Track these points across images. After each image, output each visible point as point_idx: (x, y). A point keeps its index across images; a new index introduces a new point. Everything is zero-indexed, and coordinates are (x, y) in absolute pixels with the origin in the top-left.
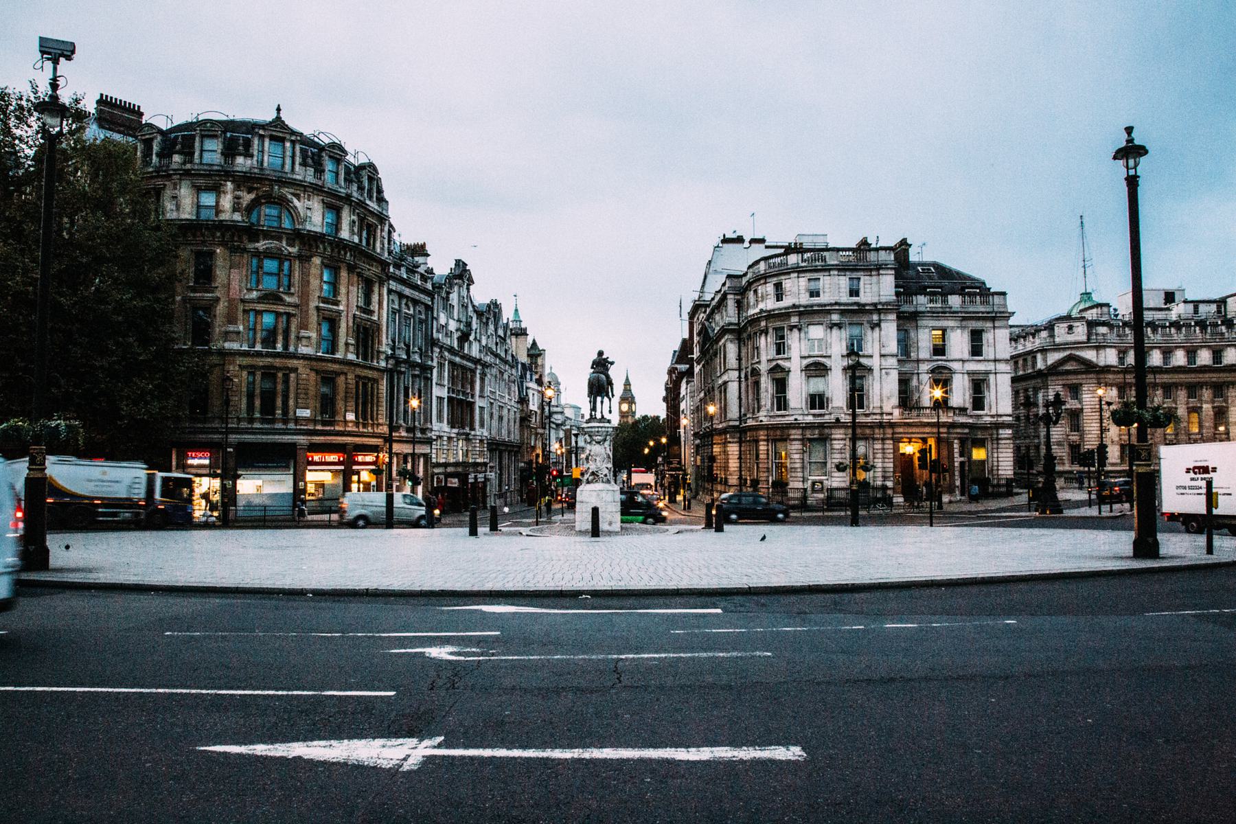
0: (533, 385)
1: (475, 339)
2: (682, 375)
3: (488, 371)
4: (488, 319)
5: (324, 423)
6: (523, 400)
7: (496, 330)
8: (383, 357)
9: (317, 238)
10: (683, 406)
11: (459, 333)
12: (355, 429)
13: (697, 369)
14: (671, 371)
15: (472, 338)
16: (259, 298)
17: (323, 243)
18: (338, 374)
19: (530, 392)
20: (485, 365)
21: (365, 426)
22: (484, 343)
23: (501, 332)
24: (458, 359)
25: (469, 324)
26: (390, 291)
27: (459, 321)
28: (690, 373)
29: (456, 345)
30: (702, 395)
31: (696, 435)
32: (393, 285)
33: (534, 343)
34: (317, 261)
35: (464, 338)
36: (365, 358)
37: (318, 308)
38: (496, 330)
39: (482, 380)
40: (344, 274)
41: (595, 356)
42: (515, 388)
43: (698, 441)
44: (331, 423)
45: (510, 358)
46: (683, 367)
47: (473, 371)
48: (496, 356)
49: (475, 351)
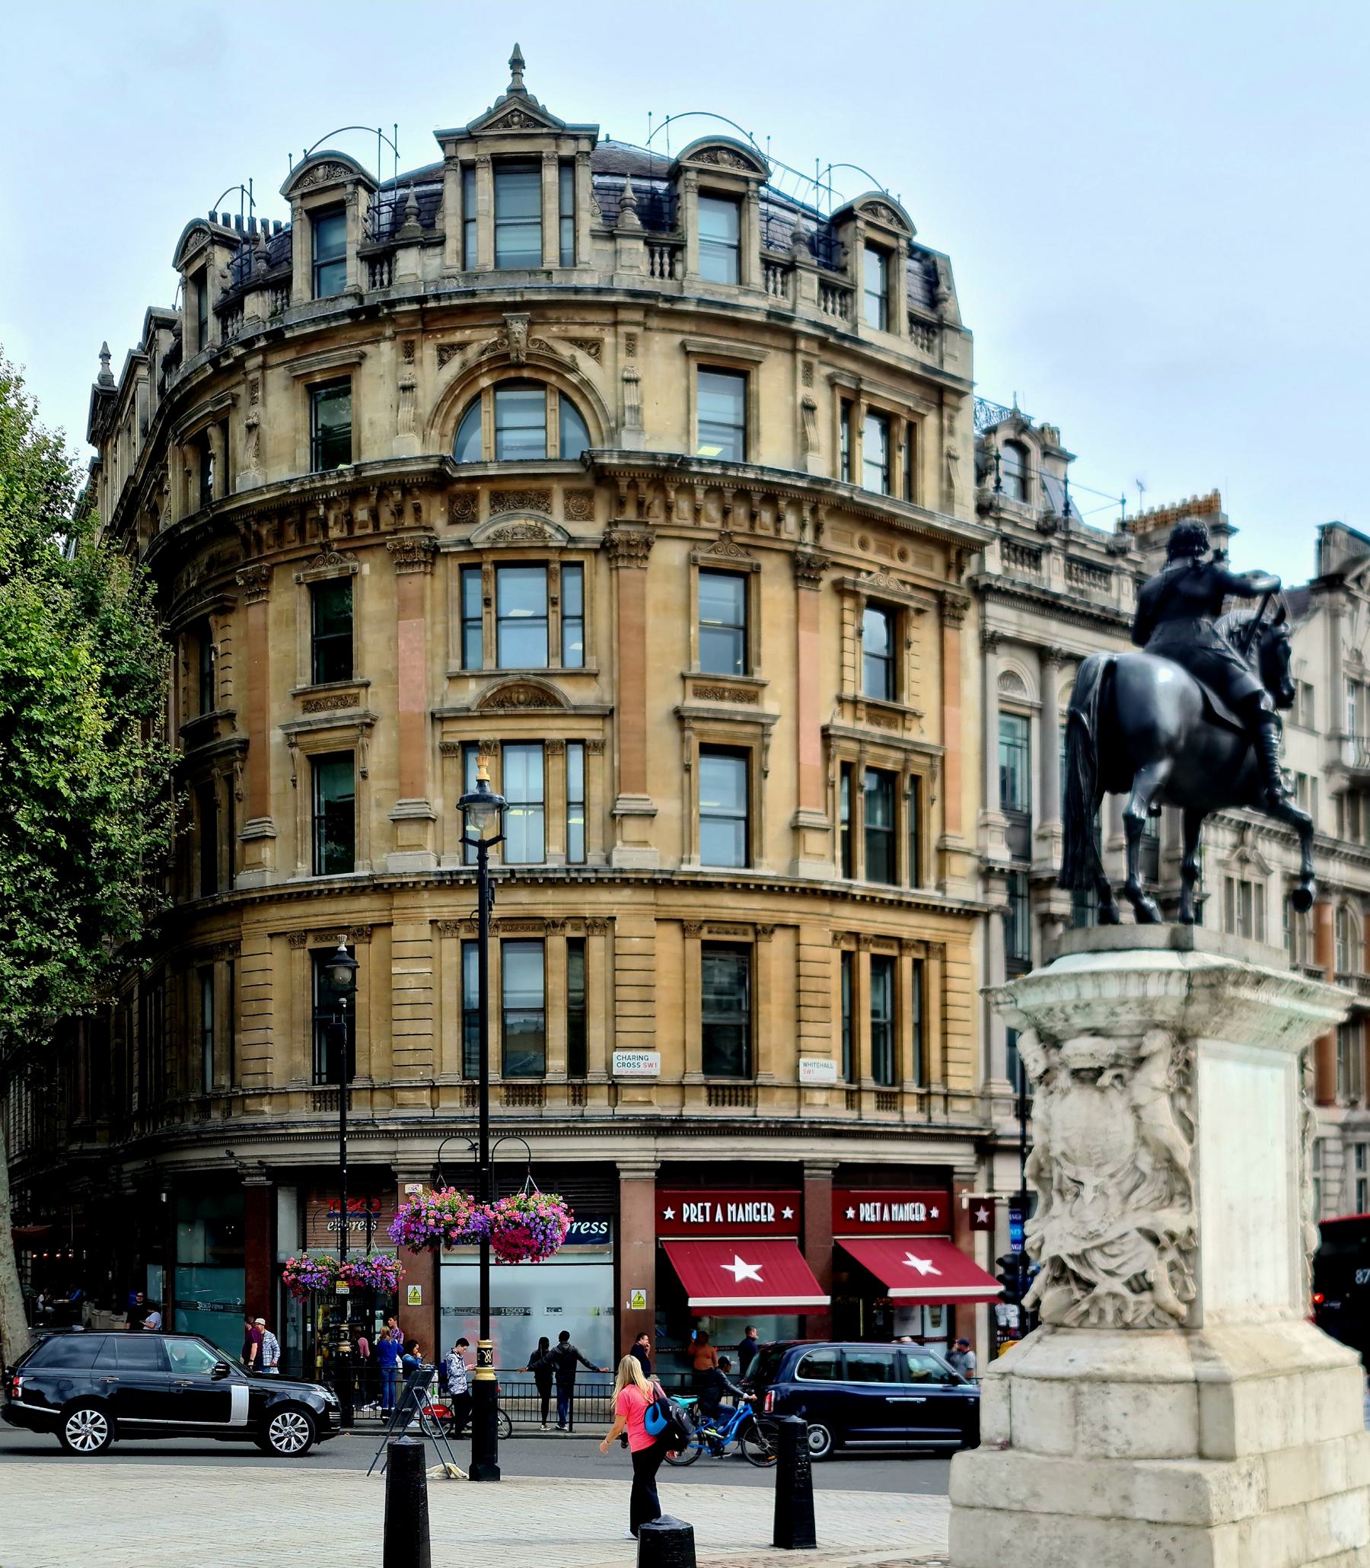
5: (717, 1095)
8: (961, 867)
9: (669, 474)
11: (1341, 782)
12: (839, 1111)
16: (485, 702)
17: (688, 489)
18: (765, 931)
21: (888, 1100)
26: (990, 642)
32: (1004, 618)
34: (669, 555)
36: (886, 868)
37: (680, 717)
40: (775, 590)
44: (742, 1095)
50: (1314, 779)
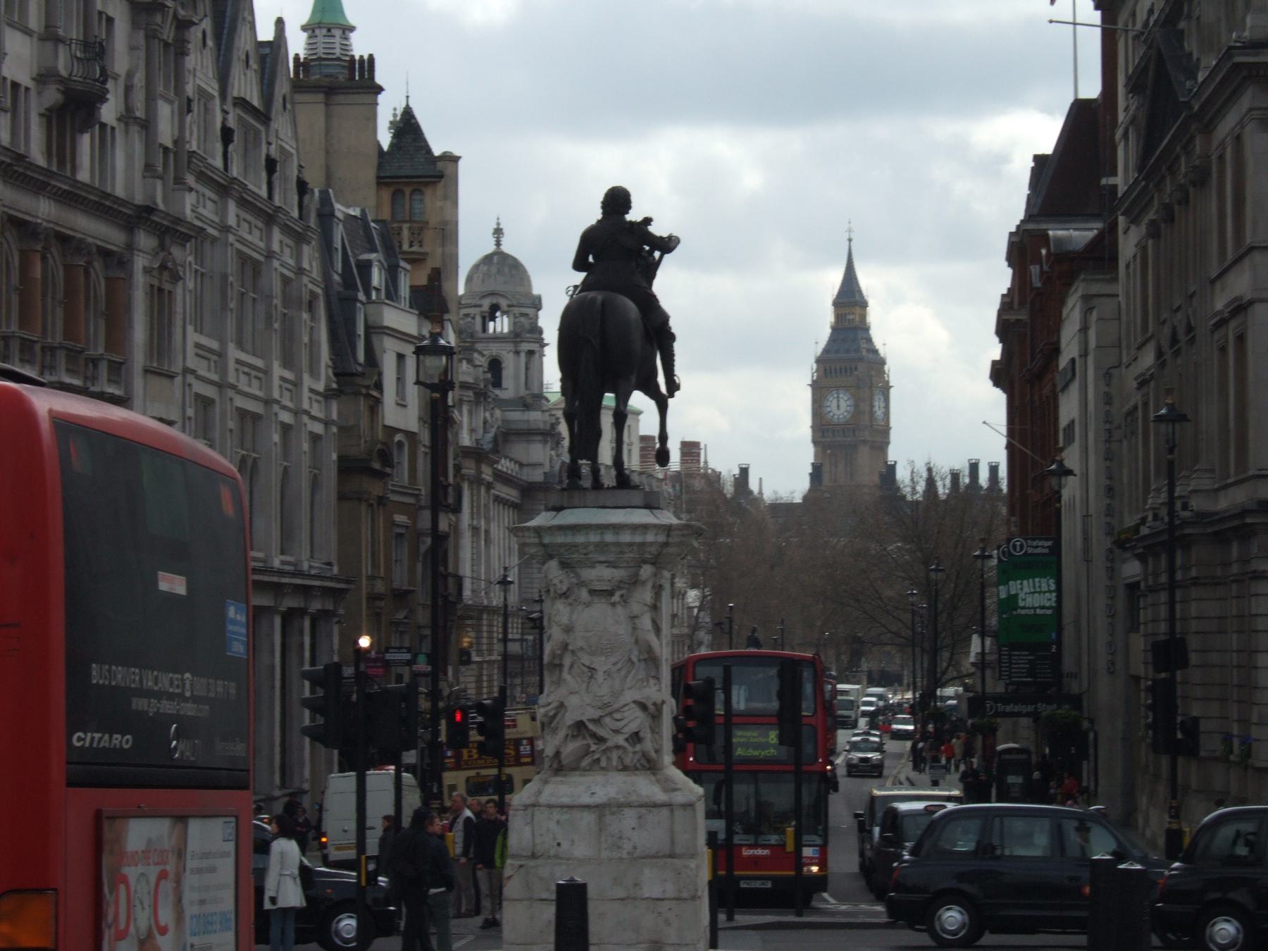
0: (401, 319)
1: (127, 117)
2: (1068, 266)
3: (182, 255)
4: (183, 25)
6: (354, 380)
7: (223, 78)
10: (1069, 408)
11: (52, 95)
13: (1128, 245)
14: (1022, 249)
15: (109, 112)
19: (389, 351)
20: (173, 231)
22: (165, 132)
23: (246, 85)
24: (44, 210)
25: (95, 51)
27: (50, 36)
28: (1100, 256)
29: (37, 155)
30: (1148, 359)
31: (1123, 543)
33: (407, 126)
35: (75, 109)
38: (223, 78)
39: (160, 299)
41: (594, 214)
42: (316, 331)
43: (1132, 569)
45: (286, 199)
46: (1077, 235)
47: (117, 261)
48: (225, 188)
49: (125, 175)
50: (27, 89)
